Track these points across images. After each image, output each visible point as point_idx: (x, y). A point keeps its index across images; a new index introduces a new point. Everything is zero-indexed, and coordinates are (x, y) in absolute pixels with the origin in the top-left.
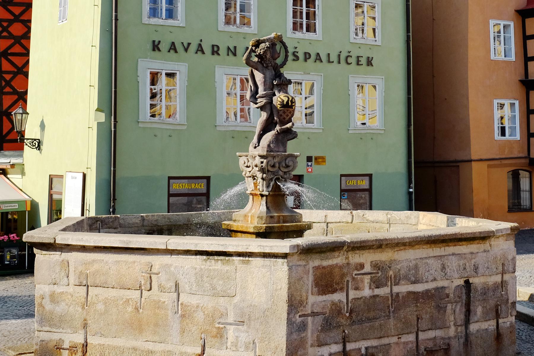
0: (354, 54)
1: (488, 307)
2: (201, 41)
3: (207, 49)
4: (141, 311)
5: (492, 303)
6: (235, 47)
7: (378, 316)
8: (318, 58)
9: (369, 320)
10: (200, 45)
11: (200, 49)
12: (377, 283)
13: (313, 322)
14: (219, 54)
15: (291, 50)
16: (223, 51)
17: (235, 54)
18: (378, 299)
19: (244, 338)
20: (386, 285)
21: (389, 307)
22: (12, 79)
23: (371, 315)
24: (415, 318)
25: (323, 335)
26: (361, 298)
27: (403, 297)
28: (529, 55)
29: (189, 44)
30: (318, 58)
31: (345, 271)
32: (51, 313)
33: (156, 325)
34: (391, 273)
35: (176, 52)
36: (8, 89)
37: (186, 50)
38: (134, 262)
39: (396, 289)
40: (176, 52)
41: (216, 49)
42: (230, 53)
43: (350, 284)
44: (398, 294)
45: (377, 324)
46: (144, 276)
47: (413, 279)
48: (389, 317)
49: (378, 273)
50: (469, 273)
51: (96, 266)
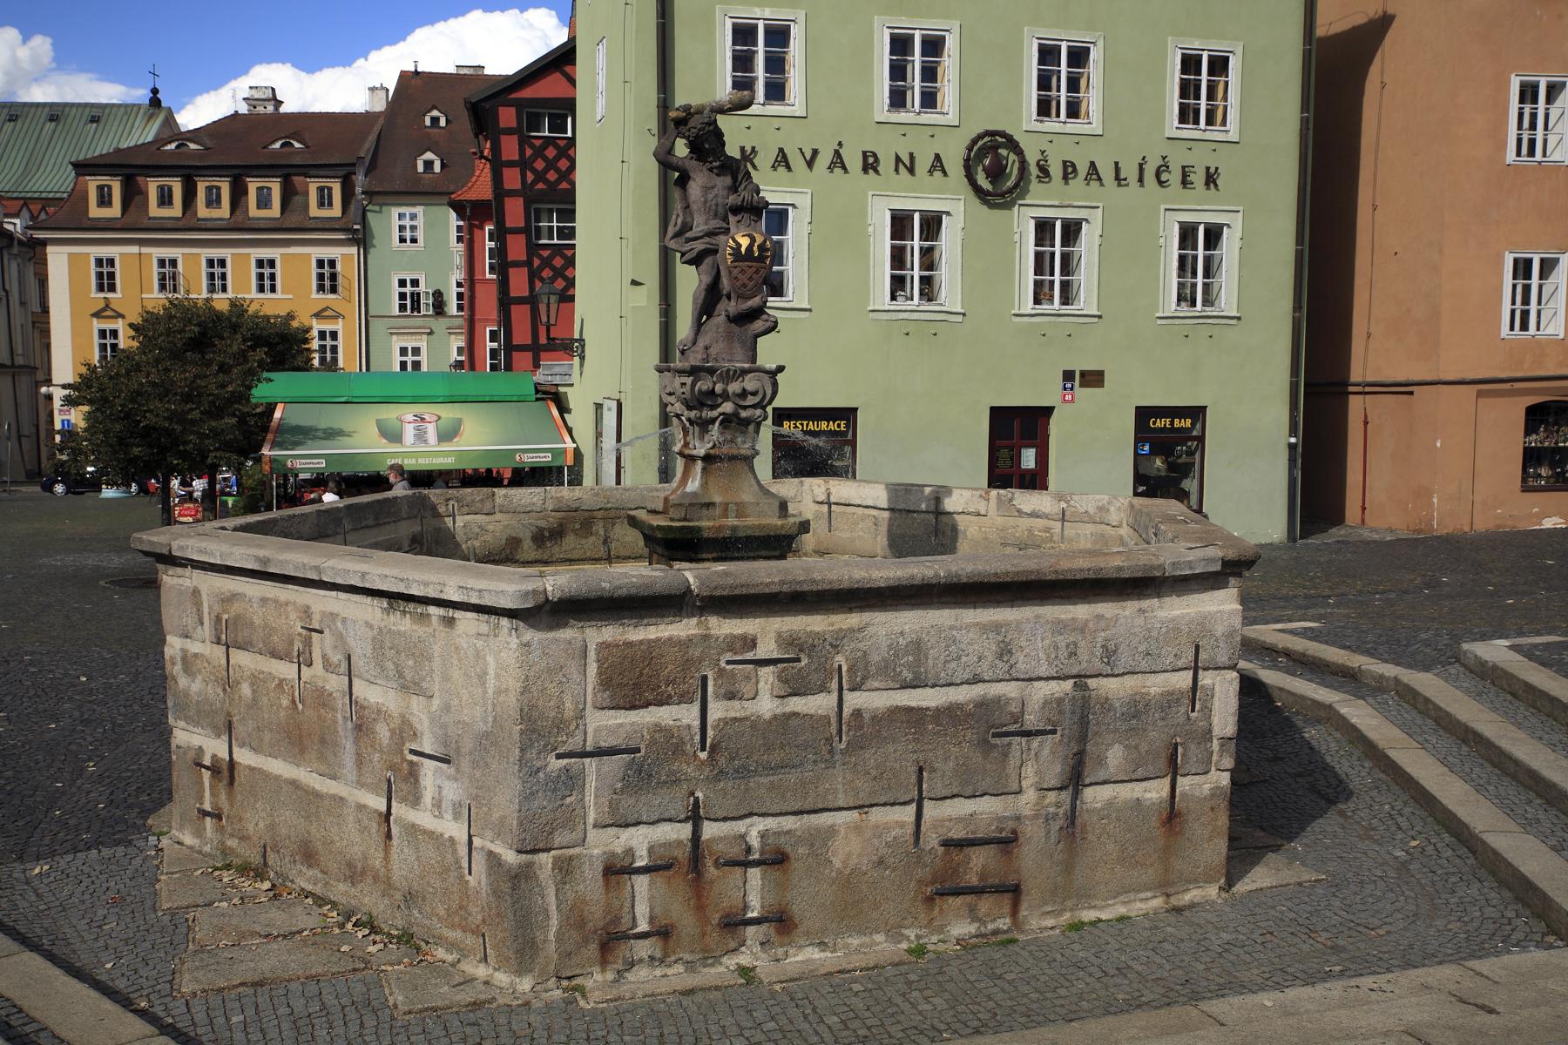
1: (1144, 747)
2: (840, 144)
3: (854, 161)
4: (300, 706)
5: (1156, 737)
7: (796, 761)
9: (770, 769)
10: (837, 153)
11: (838, 161)
12: (795, 687)
13: (598, 770)
14: (877, 172)
15: (1032, 157)
16: (887, 164)
17: (911, 170)
18: (793, 722)
19: (452, 792)
20: (823, 689)
21: (829, 740)
23: (777, 757)
24: (913, 769)
25: (627, 802)
26: (746, 718)
27: (874, 718)
29: (815, 152)
31: (696, 652)
33: (323, 741)
34: (840, 659)
35: (788, 168)
37: (810, 164)
39: (853, 700)
40: (788, 168)
41: (871, 160)
42: (901, 167)
43: (710, 683)
44: (857, 713)
45: (792, 777)
47: (908, 675)
48: (830, 764)
49: (798, 660)
50: (1085, 665)
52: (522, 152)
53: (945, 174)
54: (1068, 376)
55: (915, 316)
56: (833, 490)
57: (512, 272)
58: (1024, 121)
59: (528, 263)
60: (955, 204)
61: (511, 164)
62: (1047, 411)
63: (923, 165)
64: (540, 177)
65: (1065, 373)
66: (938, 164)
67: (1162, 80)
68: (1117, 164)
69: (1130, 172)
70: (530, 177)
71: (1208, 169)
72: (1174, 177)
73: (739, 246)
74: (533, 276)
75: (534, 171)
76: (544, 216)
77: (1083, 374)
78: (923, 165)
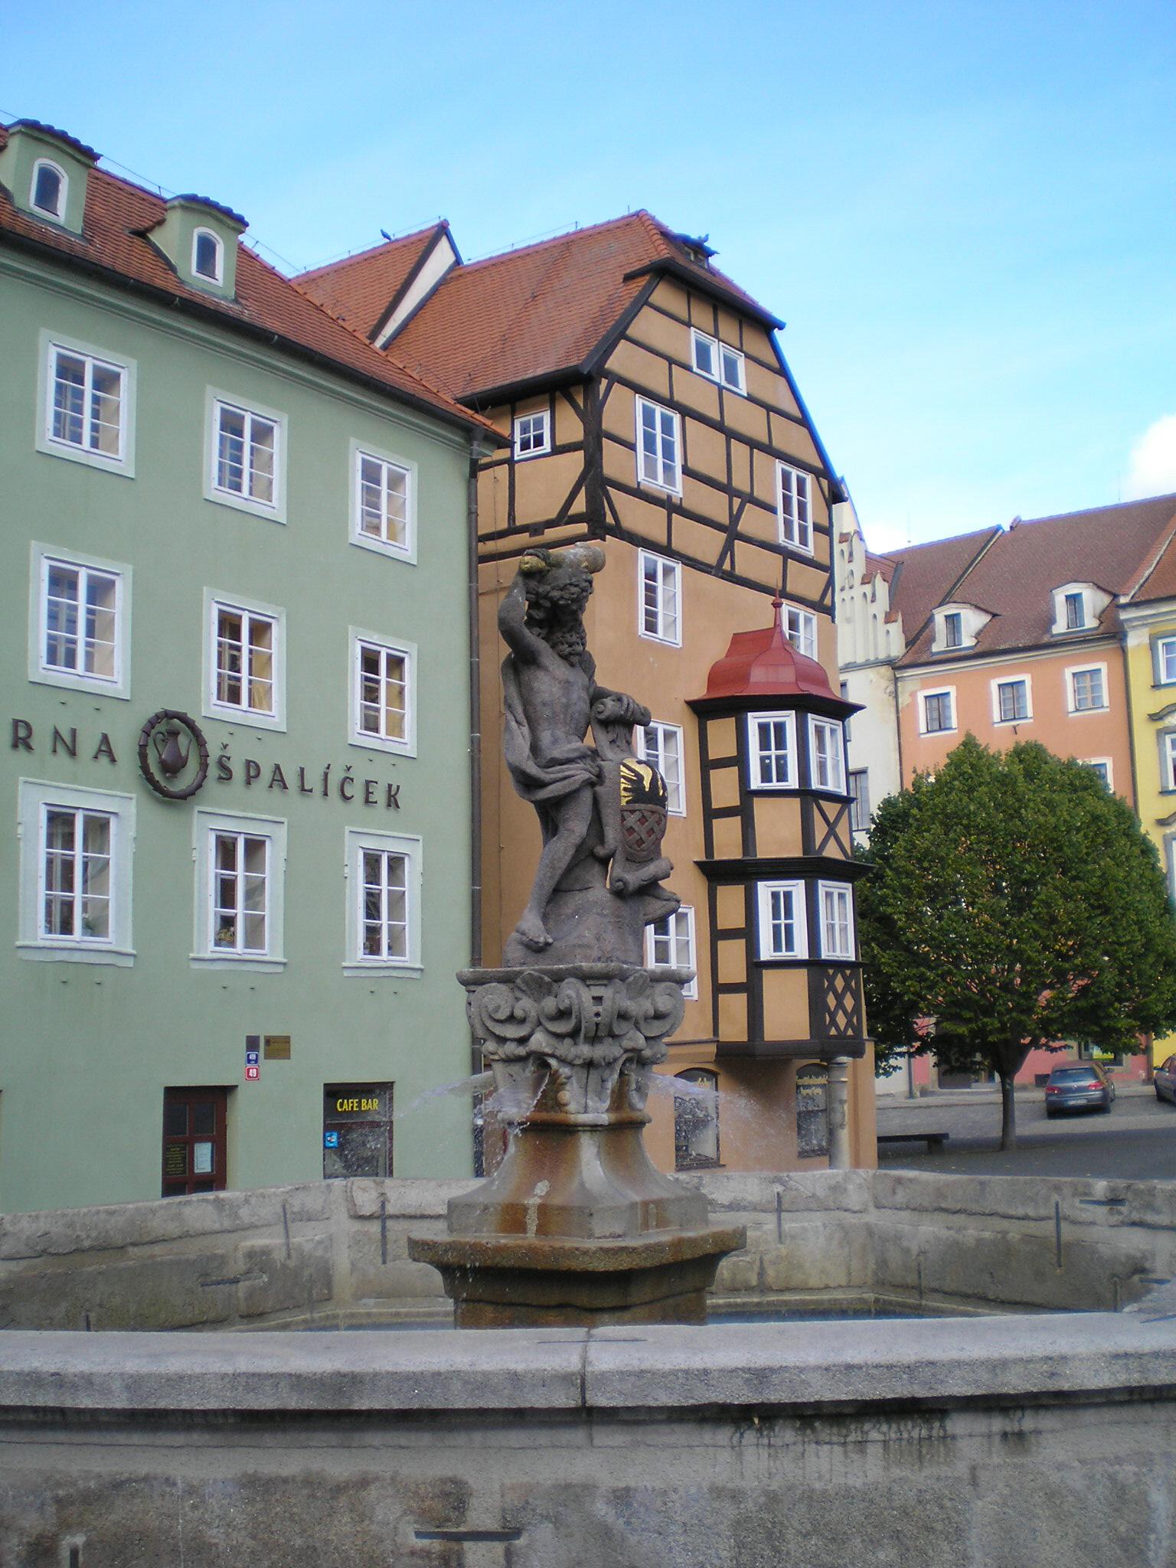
0: (359, 776)
6: (74, 732)
8: (278, 779)
14: (29, 748)
15: (214, 752)
16: (42, 739)
17: (72, 753)
28: (716, 805)
30: (277, 777)
38: (364, 1483)
41: (22, 733)
42: (60, 749)
46: (426, 1554)
51: (118, 1515)
53: (113, 761)
54: (252, 1043)
55: (77, 957)
56: (392, 1196)
58: (209, 707)
60: (125, 806)
62: (221, 1095)
63: (88, 745)
65: (286, 1040)
66: (105, 749)
67: (343, 674)
68: (302, 770)
69: (313, 780)
71: (390, 786)
72: (356, 790)
73: (640, 778)
77: (268, 1041)
78: (88, 745)
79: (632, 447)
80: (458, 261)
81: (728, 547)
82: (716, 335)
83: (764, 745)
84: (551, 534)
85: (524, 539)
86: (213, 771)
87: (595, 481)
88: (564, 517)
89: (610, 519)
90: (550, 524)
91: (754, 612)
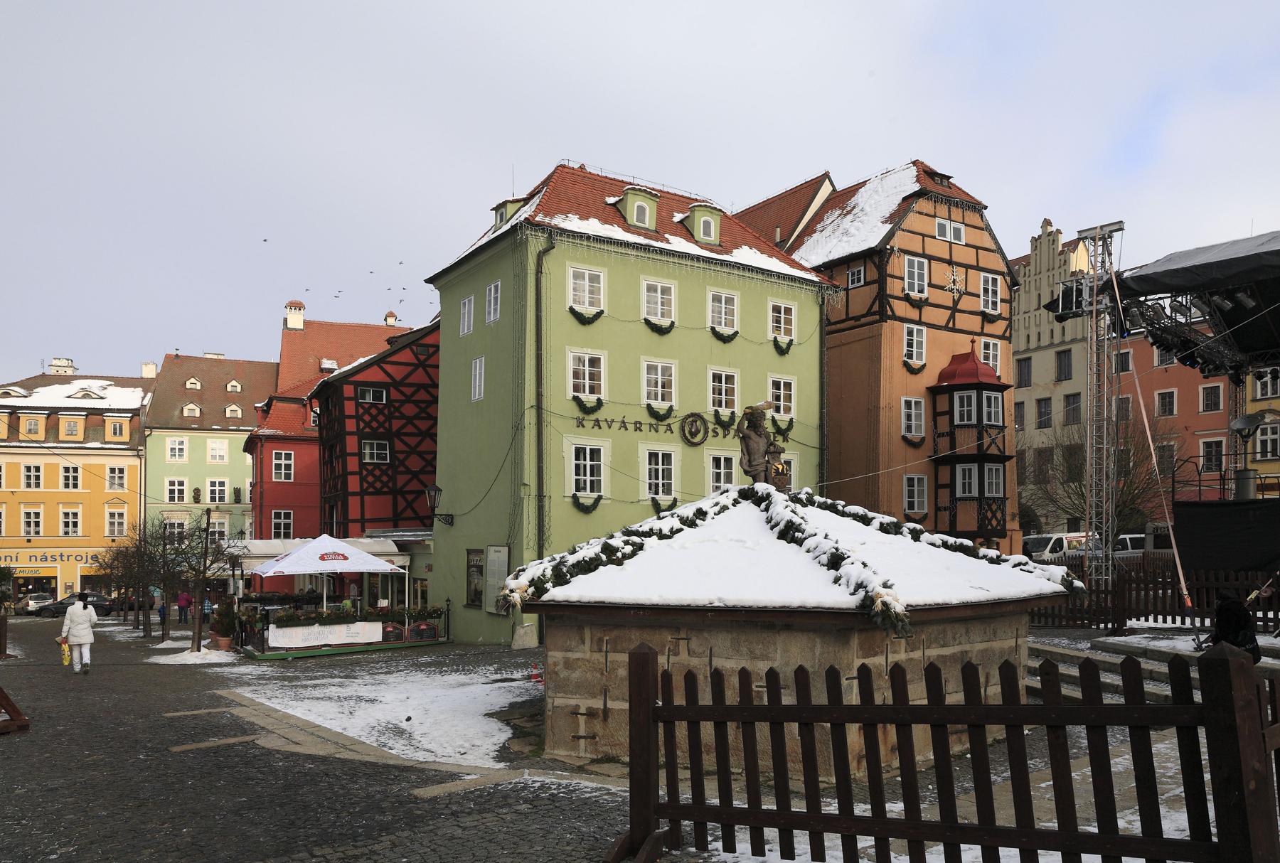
22: (405, 459)
32: (567, 679)
36: (402, 469)
52: (357, 411)
57: (350, 478)
59: (360, 473)
60: (677, 449)
61: (350, 417)
64: (368, 424)
70: (362, 425)
74: (363, 480)
75: (364, 421)
76: (367, 447)
79: (902, 279)
80: (834, 189)
81: (952, 317)
82: (950, 219)
83: (962, 405)
84: (863, 320)
85: (852, 323)
86: (711, 434)
87: (882, 297)
88: (869, 313)
89: (889, 313)
90: (863, 316)
91: (961, 344)
